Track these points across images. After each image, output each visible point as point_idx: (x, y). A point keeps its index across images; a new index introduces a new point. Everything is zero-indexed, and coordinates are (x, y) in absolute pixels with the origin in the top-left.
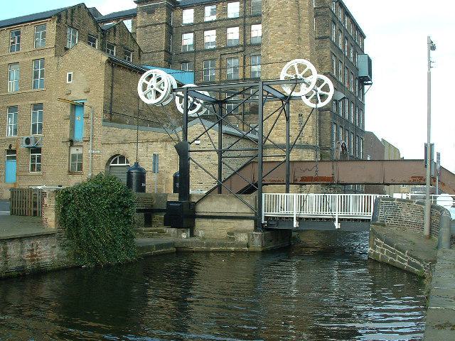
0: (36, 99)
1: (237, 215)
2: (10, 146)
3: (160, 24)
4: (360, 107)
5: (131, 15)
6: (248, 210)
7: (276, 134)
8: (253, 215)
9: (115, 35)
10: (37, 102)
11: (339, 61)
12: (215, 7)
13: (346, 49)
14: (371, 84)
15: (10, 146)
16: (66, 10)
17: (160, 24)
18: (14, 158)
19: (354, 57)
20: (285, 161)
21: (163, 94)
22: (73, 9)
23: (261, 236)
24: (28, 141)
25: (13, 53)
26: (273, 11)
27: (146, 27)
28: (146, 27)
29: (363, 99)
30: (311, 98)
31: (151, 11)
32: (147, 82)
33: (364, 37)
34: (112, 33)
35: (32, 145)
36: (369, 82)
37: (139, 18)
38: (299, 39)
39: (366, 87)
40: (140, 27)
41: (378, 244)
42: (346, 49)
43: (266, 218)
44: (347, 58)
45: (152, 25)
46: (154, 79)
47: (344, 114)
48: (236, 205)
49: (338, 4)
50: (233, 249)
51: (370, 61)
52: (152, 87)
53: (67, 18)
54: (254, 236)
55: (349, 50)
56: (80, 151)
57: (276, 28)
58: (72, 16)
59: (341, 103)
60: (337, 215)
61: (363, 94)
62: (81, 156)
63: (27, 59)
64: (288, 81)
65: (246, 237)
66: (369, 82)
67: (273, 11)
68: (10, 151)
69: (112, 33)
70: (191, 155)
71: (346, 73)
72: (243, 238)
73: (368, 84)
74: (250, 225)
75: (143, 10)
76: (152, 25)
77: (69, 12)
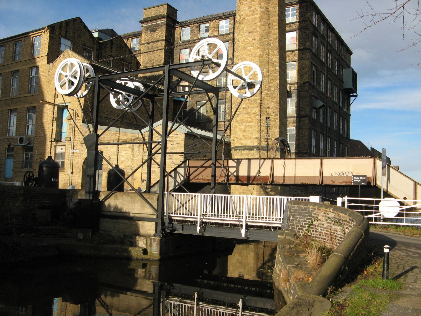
0: (31, 103)
2: (9, 145)
3: (160, 41)
4: (346, 117)
5: (137, 35)
7: (243, 136)
9: (112, 48)
10: (32, 105)
11: (319, 72)
12: (208, 25)
13: (329, 62)
14: (356, 96)
15: (9, 145)
16: (61, 23)
17: (160, 41)
18: (12, 156)
19: (339, 70)
21: (76, 82)
22: (67, 22)
24: (21, 140)
25: (14, 62)
26: (244, 19)
27: (148, 43)
28: (148, 43)
29: (349, 109)
30: (238, 88)
31: (153, 30)
33: (351, 53)
34: (109, 46)
35: (25, 143)
36: (355, 94)
37: (143, 35)
38: (269, 44)
39: (352, 99)
40: (144, 44)
42: (329, 62)
44: (331, 70)
45: (154, 42)
47: (326, 121)
48: (139, 204)
49: (320, 19)
51: (355, 75)
53: (61, 29)
54: (153, 241)
55: (333, 64)
56: (63, 151)
57: (246, 34)
58: (66, 28)
59: (322, 111)
60: (244, 220)
61: (349, 105)
62: (63, 154)
63: (25, 67)
66: (355, 94)
67: (244, 19)
68: (10, 149)
69: (109, 46)
71: (329, 84)
73: (353, 96)
75: (147, 28)
76: (154, 42)
77: (64, 25)
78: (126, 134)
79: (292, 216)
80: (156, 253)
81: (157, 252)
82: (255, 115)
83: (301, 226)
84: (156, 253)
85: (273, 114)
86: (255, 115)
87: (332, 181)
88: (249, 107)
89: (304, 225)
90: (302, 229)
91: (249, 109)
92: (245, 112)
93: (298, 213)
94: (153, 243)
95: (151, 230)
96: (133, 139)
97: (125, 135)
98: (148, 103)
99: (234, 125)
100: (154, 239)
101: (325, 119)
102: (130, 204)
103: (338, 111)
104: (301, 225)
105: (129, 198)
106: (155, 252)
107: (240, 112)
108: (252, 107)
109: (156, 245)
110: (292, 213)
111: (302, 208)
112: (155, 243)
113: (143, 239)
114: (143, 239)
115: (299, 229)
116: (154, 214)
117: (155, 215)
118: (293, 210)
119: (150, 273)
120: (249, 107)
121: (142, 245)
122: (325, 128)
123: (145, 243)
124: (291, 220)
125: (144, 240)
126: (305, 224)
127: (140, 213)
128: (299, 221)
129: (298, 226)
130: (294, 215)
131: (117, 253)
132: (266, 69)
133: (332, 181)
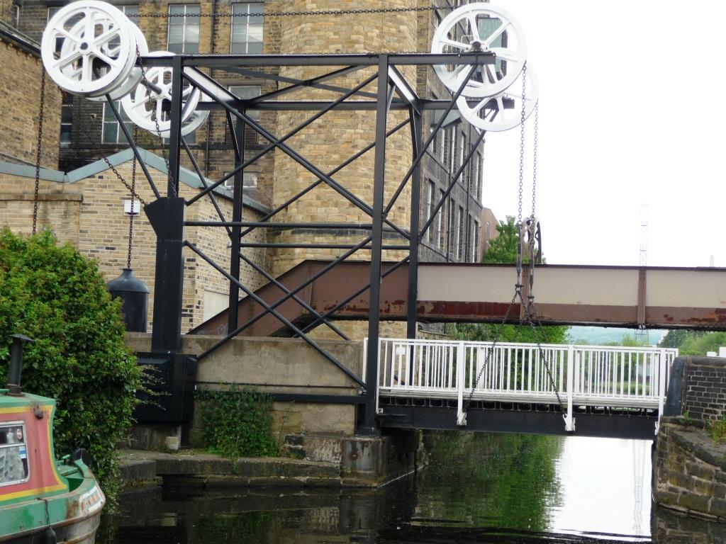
1: (309, 391)
6: (340, 380)
7: (318, 198)
8: (352, 393)
20: (404, 262)
23: (374, 447)
32: (64, 33)
41: (694, 471)
43: (385, 400)
46: (87, 25)
48: (307, 364)
50: (303, 479)
52: (84, 46)
54: (359, 446)
64: (452, 58)
65: (337, 448)
70: (188, 233)
72: (327, 454)
74: (342, 418)
78: (20, 178)
79: (691, 386)
80: (368, 472)
81: (370, 470)
82: (351, 145)
83: (711, 406)
84: (368, 472)
85: (393, 146)
86: (351, 145)
87: (666, 316)
88: (336, 125)
89: (717, 404)
90: (715, 412)
91: (333, 130)
92: (323, 136)
93: (704, 379)
94: (360, 451)
95: (343, 423)
96: (47, 195)
97: (17, 182)
98: (8, 88)
99: (288, 166)
100: (363, 443)
101: (448, 153)
102: (283, 366)
103: (467, 133)
104: (713, 403)
105: (278, 352)
106: (366, 470)
107: (308, 136)
108: (343, 126)
109: (369, 454)
110: (691, 381)
111: (713, 370)
112: (367, 451)
113: (334, 444)
114: (334, 444)
115: (707, 411)
116: (350, 385)
117: (352, 388)
118: (692, 374)
119: (352, 514)
120: (336, 125)
121: (330, 455)
122: (447, 176)
123: (340, 450)
124: (690, 393)
125: (336, 445)
126: (719, 401)
127: (311, 385)
128: (705, 395)
129: (706, 405)
130: (695, 384)
131: (282, 477)
132: (377, 28)
133: (666, 316)
